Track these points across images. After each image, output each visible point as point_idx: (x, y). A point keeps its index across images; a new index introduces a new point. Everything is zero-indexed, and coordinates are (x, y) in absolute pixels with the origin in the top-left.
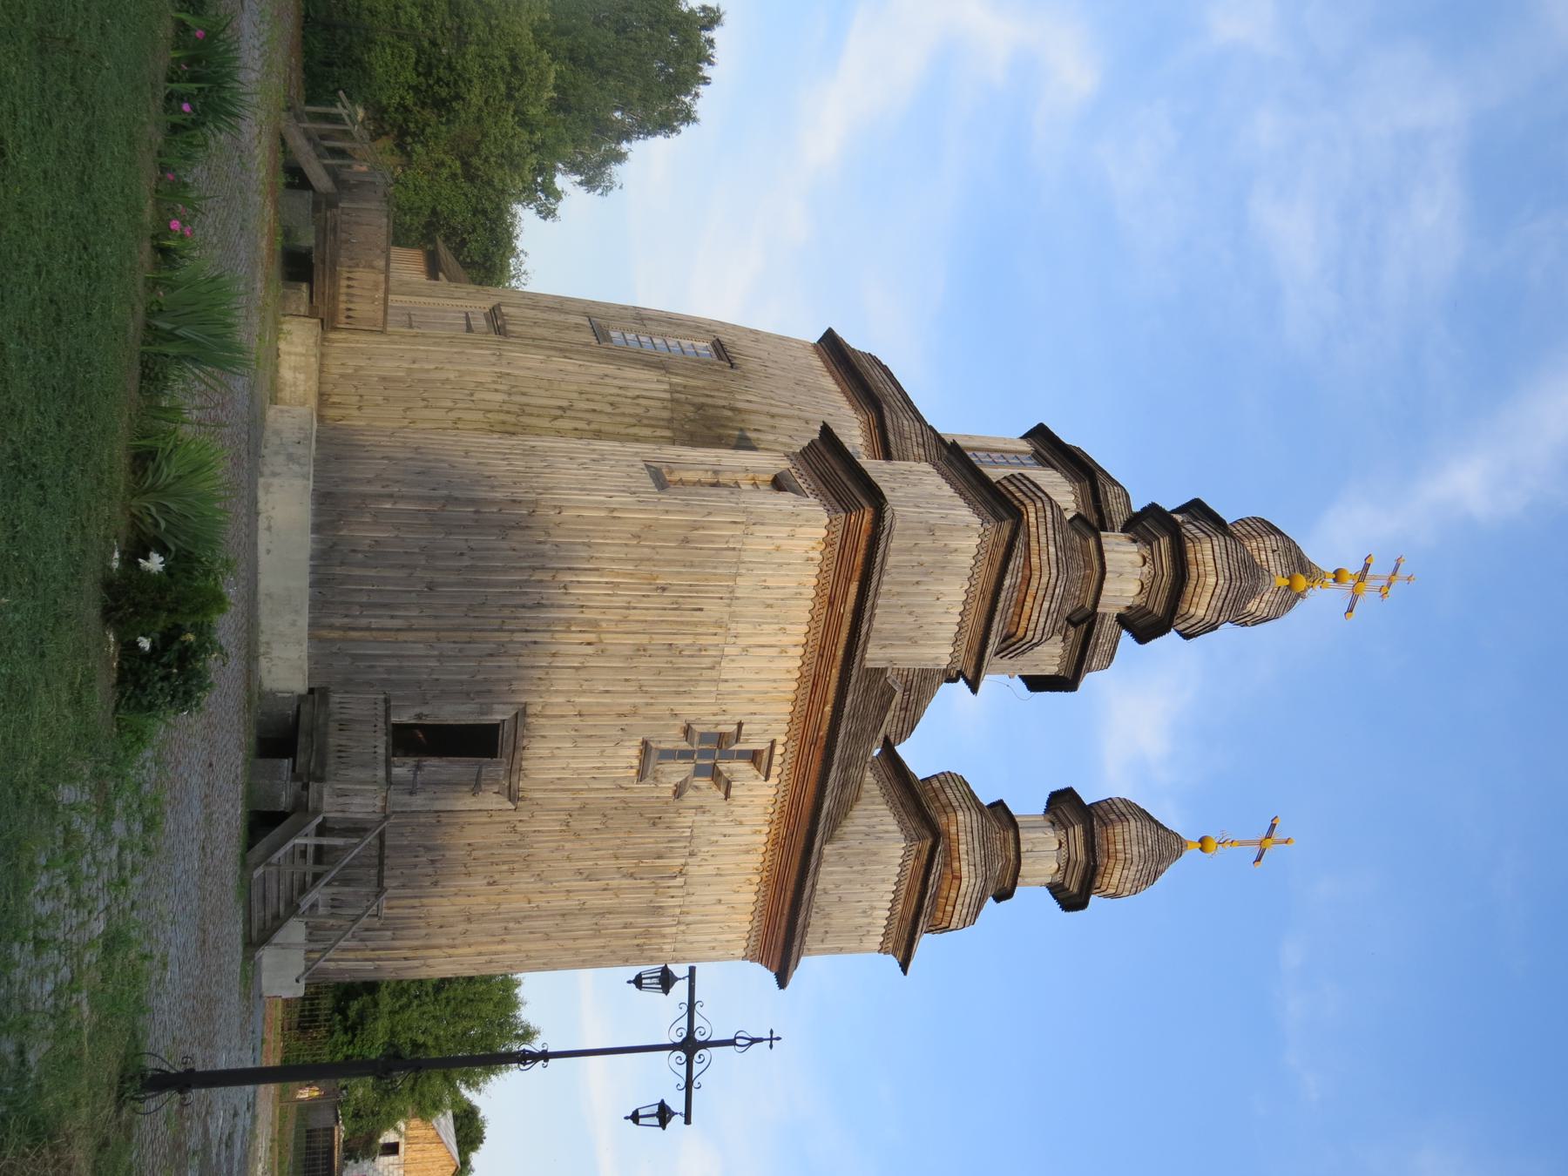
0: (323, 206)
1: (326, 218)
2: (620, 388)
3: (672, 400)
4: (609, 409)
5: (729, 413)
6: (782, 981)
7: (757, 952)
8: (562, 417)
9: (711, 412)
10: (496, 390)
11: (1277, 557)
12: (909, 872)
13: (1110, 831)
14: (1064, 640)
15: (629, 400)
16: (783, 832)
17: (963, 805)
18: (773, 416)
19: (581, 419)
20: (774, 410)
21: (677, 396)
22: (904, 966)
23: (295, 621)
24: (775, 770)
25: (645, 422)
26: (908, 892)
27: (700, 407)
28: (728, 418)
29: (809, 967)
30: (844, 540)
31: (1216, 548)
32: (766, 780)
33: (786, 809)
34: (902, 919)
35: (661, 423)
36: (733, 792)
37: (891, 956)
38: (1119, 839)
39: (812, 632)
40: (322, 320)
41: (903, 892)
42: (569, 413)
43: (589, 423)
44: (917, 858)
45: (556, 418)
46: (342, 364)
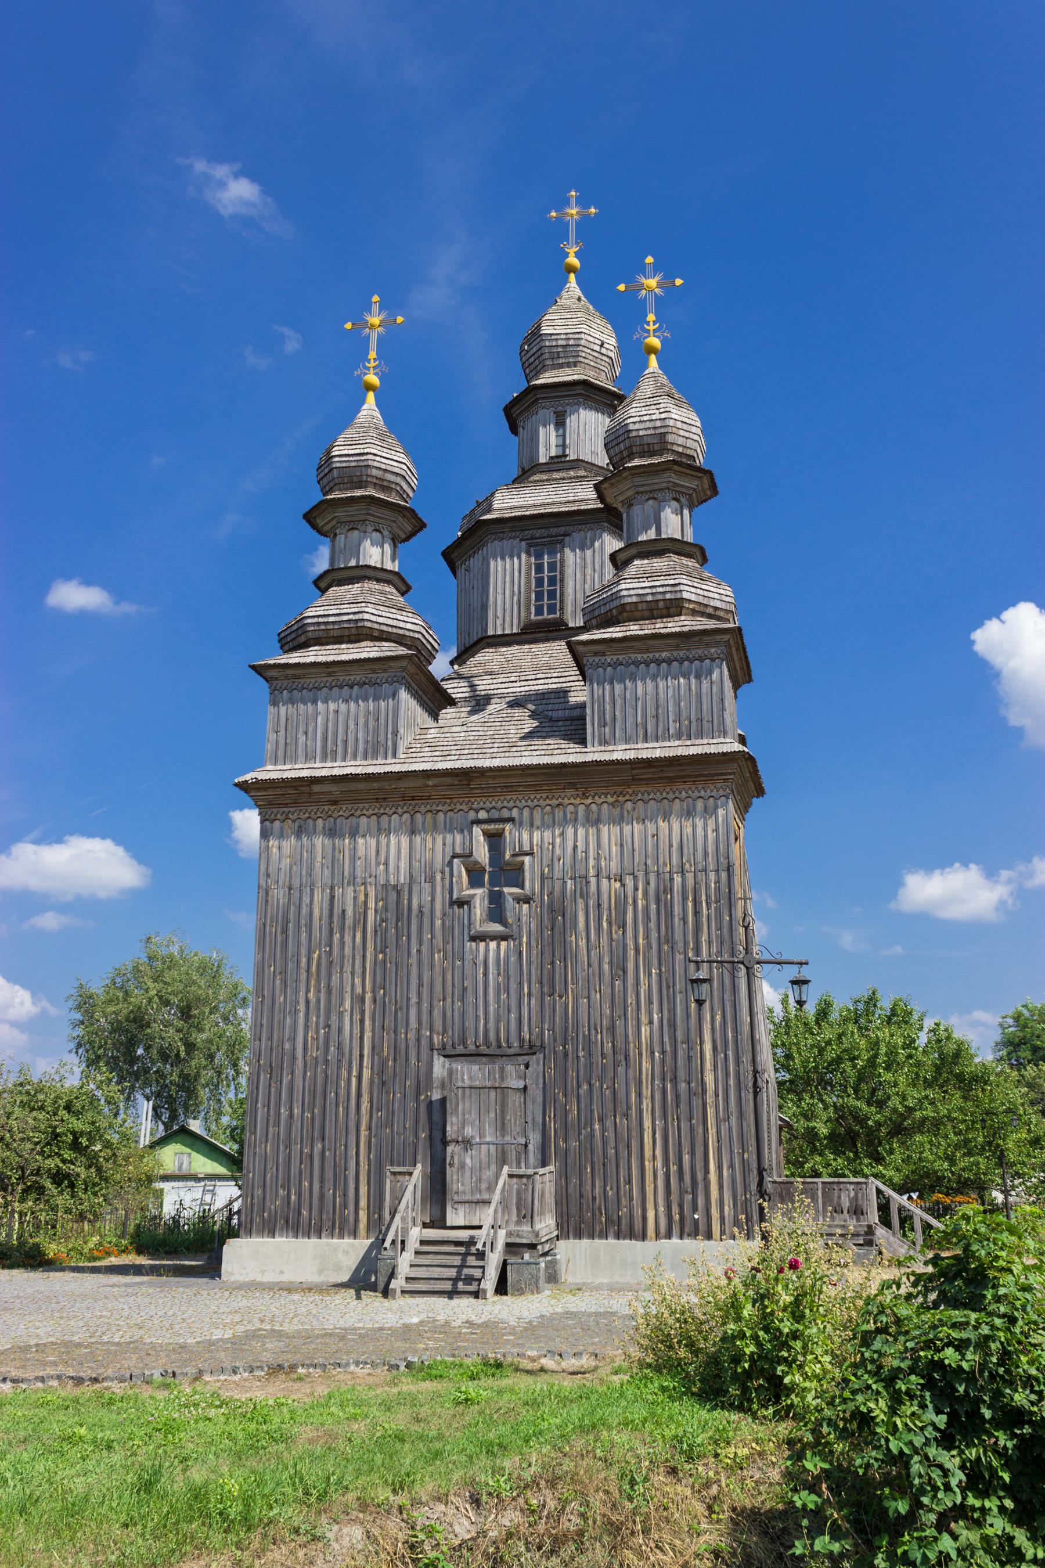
7: (719, 785)
12: (621, 657)
14: (569, 535)
16: (570, 792)
23: (344, 1251)
24: (505, 814)
26: (647, 651)
30: (280, 805)
33: (544, 795)
39: (365, 812)
41: (645, 656)
44: (603, 654)
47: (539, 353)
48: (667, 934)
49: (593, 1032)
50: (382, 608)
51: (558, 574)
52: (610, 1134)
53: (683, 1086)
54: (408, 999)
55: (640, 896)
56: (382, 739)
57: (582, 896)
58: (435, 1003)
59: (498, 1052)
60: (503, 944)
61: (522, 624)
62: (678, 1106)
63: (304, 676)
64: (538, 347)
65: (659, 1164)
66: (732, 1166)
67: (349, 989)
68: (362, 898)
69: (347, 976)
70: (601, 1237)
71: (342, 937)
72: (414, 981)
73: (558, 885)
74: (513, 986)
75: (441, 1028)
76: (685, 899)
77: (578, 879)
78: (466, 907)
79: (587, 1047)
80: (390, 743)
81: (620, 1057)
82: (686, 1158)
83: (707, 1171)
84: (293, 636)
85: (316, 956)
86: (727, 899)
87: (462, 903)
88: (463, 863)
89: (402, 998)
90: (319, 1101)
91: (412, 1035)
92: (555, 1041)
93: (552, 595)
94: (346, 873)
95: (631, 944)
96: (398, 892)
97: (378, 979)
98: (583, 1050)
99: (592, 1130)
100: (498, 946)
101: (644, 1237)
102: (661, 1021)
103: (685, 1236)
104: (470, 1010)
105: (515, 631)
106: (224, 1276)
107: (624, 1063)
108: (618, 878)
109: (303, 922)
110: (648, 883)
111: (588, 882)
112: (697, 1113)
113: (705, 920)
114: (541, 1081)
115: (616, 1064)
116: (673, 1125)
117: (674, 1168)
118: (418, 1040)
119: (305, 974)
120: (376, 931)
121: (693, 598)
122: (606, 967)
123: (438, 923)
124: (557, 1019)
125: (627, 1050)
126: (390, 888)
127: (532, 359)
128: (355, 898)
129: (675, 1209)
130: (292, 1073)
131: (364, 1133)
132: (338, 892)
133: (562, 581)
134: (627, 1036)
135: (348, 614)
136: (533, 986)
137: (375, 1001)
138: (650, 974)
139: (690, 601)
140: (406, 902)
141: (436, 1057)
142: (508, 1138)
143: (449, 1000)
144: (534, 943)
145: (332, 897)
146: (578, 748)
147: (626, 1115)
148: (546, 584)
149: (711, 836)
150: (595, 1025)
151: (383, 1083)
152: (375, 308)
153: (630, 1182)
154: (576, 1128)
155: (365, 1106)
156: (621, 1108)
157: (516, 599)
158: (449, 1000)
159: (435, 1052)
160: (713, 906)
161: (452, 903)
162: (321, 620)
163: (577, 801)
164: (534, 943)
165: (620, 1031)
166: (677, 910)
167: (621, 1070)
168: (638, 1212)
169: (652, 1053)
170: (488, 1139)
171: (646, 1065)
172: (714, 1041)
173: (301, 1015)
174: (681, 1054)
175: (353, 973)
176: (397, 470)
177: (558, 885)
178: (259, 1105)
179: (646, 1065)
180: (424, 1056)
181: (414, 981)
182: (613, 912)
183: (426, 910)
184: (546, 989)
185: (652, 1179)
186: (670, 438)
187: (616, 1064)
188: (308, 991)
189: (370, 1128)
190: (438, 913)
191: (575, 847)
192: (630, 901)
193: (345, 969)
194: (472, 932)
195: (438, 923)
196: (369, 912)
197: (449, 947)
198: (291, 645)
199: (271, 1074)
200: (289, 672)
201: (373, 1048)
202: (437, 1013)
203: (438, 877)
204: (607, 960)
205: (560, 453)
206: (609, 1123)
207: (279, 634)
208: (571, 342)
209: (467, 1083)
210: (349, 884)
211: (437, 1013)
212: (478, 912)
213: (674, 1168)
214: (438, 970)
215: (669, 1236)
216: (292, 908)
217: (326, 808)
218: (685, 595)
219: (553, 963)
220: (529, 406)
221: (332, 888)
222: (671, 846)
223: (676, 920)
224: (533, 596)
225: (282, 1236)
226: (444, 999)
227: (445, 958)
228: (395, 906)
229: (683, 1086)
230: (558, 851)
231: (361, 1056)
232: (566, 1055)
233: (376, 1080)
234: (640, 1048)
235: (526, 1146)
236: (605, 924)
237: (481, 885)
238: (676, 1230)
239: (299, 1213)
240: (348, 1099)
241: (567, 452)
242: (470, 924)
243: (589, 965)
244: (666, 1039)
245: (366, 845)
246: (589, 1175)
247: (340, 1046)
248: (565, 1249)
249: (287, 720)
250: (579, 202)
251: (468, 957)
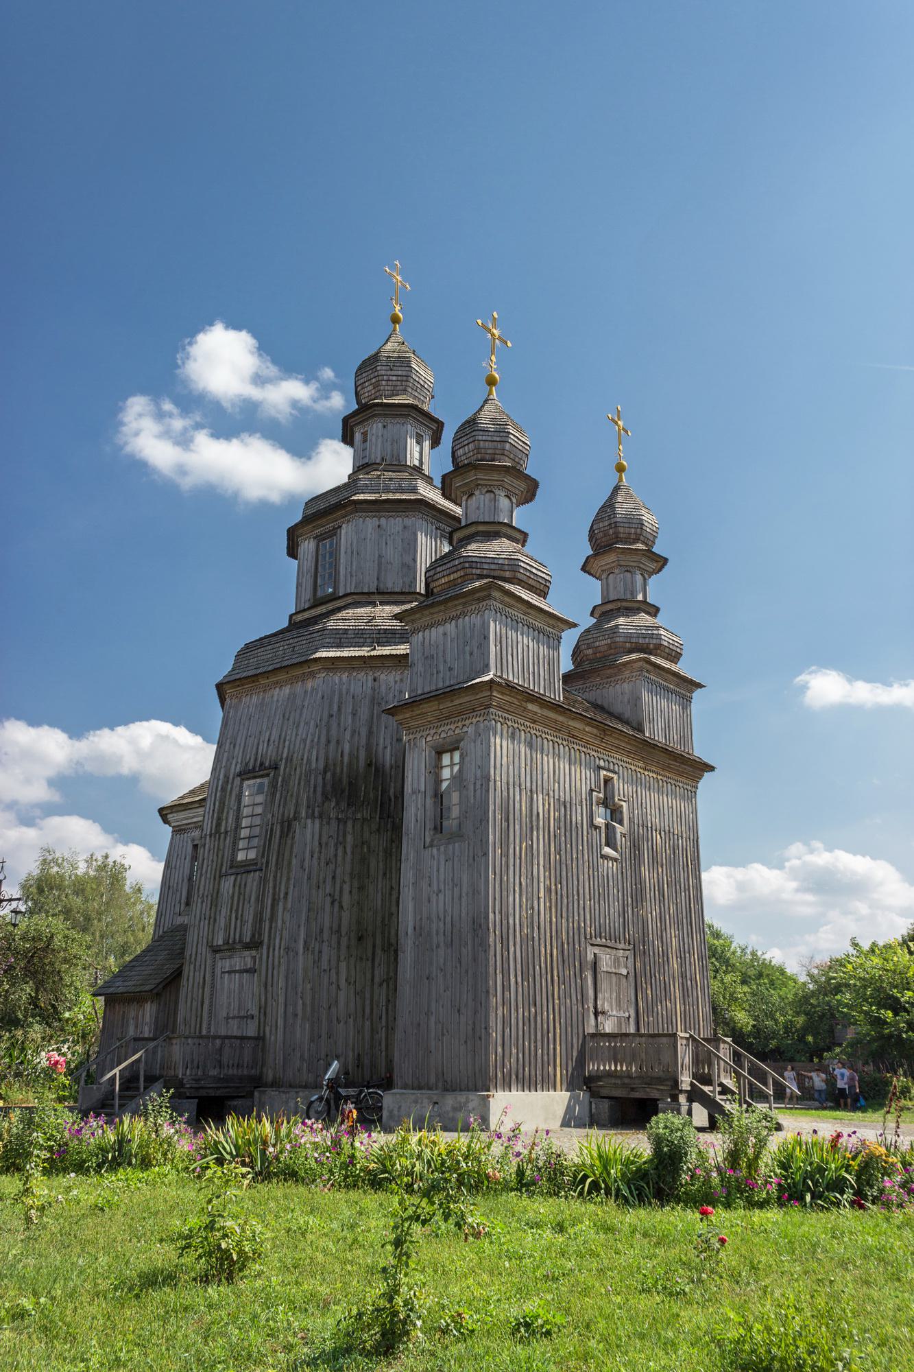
0: (182, 1090)
1: (191, 1088)
2: (312, 857)
3: (320, 817)
4: (332, 866)
5: (329, 775)
6: (712, 769)
8: (340, 903)
9: (329, 788)
10: (320, 952)
11: (395, 368)
13: (622, 535)
15: (323, 850)
17: (611, 636)
18: (328, 742)
19: (341, 888)
20: (323, 739)
21: (316, 814)
22: (699, 686)
25: (341, 839)
26: (665, 680)
27: (326, 797)
28: (334, 775)
29: (700, 751)
31: (484, 438)
34: (677, 685)
35: (341, 827)
37: (694, 695)
38: (627, 530)
40: (255, 1087)
42: (337, 897)
43: (344, 882)
45: (341, 907)
46: (299, 1071)
47: (405, 378)
63: (511, 606)
64: (404, 373)
135: (543, 572)
142: (621, 1014)
149: (691, 816)
162: (528, 568)
170: (614, 1013)
171: (675, 966)
179: (675, 966)
180: (583, 945)
189: (559, 999)
191: (642, 803)
200: (507, 599)
201: (557, 931)
208: (426, 386)
209: (605, 970)
217: (528, 724)
220: (397, 415)
235: (629, 1016)
245: (548, 762)
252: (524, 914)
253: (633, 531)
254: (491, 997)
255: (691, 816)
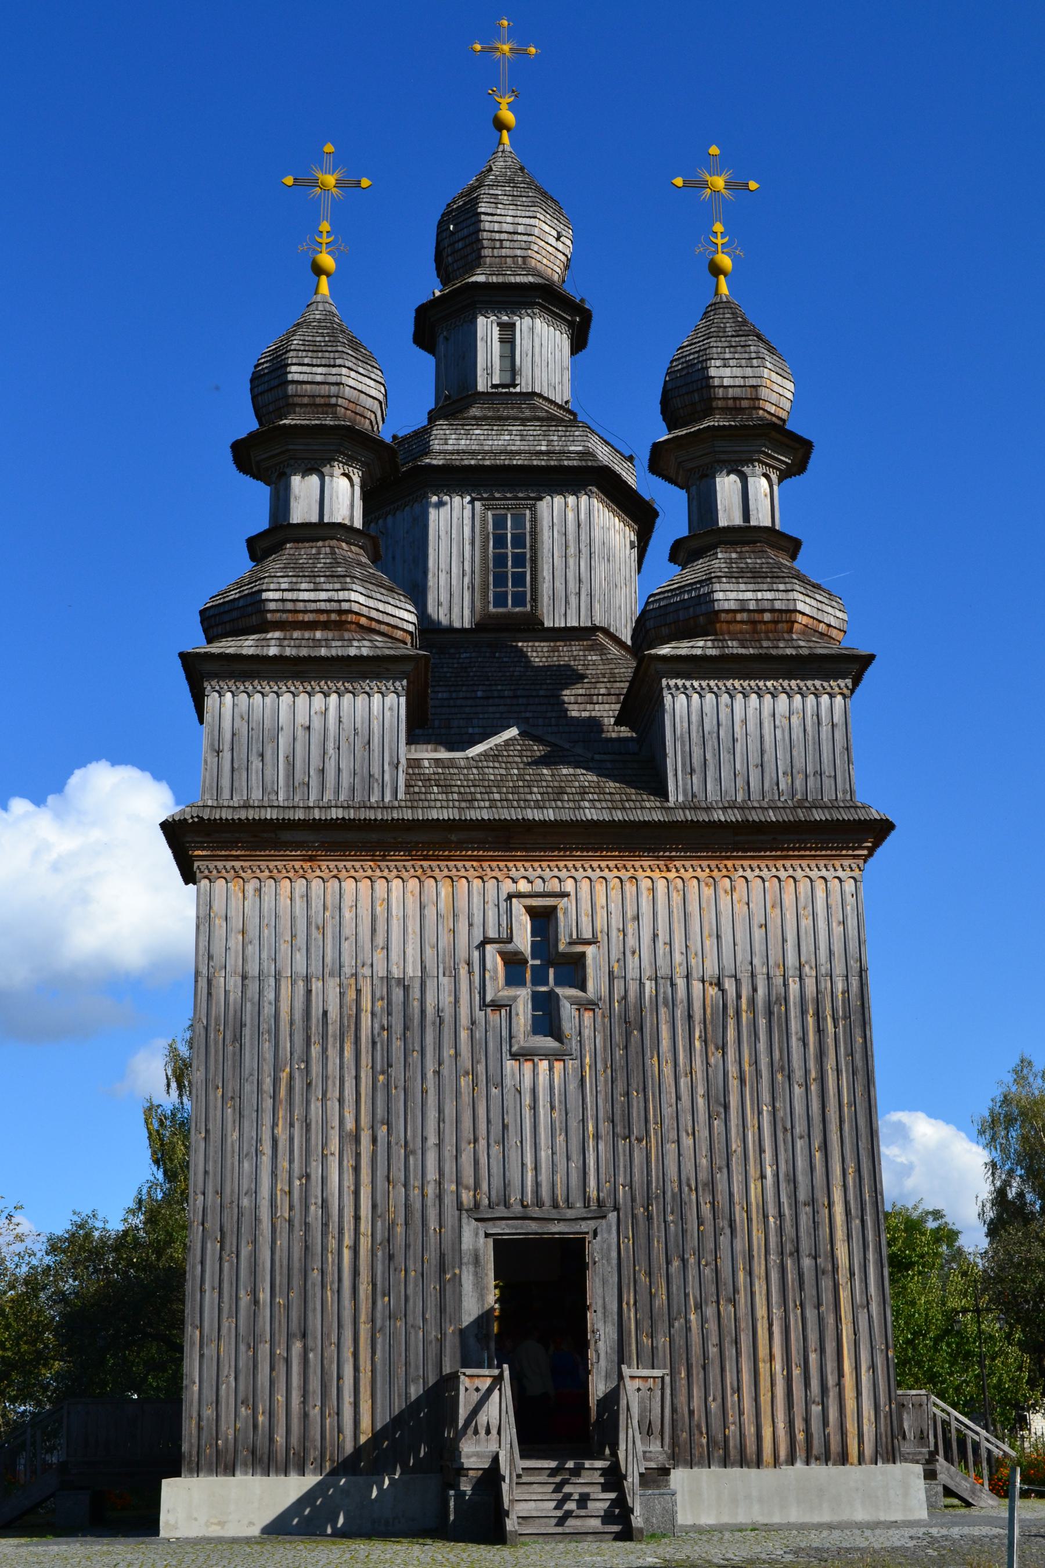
24: (554, 886)
32: (566, 895)
33: (612, 864)
36: (587, 934)
39: (352, 873)
48: (781, 1058)
49: (686, 1189)
50: (370, 586)
51: (528, 550)
52: (712, 1326)
53: (807, 1262)
54: (424, 1139)
55: (744, 1007)
56: (376, 771)
57: (666, 1005)
58: (463, 1145)
59: (554, 1214)
60: (558, 1066)
61: (477, 617)
62: (801, 1288)
65: (778, 1366)
66: (873, 1367)
67: (336, 1123)
68: (352, 995)
69: (333, 1106)
70: (700, 1464)
71: (324, 1050)
72: (432, 1115)
73: (633, 987)
74: (574, 1124)
75: (471, 1181)
76: (803, 1012)
77: (661, 981)
78: (503, 1011)
79: (677, 1210)
80: (387, 777)
81: (723, 1223)
82: (813, 1357)
83: (841, 1374)
84: (235, 614)
85: (284, 1076)
86: (859, 1016)
87: (496, 1006)
88: (501, 953)
89: (414, 1137)
90: (297, 1282)
91: (431, 1190)
92: (633, 1200)
93: (519, 580)
94: (328, 959)
95: (733, 1070)
96: (406, 989)
97: (379, 1111)
98: (672, 1213)
99: (687, 1321)
100: (551, 1069)
101: (759, 1464)
102: (777, 1175)
103: (813, 1460)
104: (514, 1156)
105: (467, 625)
106: (163, 1533)
107: (728, 1231)
108: (715, 981)
109: (264, 1026)
110: (755, 990)
111: (673, 985)
112: (827, 1297)
113: (830, 1041)
114: (614, 1254)
115: (717, 1234)
116: (796, 1316)
117: (796, 1372)
118: (440, 1197)
119: (270, 1102)
120: (374, 1043)
121: (807, 610)
122: (701, 1102)
123: (464, 1035)
124: (636, 1170)
125: (731, 1213)
126: (393, 982)
127: (460, 245)
128: (342, 995)
129: (799, 1425)
130: (255, 1242)
131: (364, 1329)
132: (316, 986)
133: (534, 561)
134: (731, 1195)
136: (601, 1126)
137: (374, 1140)
138: (760, 1113)
139: (804, 614)
140: (417, 1004)
141: (464, 1221)
143: (482, 1143)
144: (600, 1066)
145: (309, 992)
146: (651, 802)
147: (734, 1302)
148: (510, 563)
149: (838, 930)
150: (688, 1179)
151: (391, 1257)
152: (328, 161)
153: (739, 1390)
154: (666, 1318)
155: (364, 1288)
156: (726, 1291)
157: (467, 580)
158: (482, 1143)
159: (464, 1215)
160: (841, 1023)
161: (484, 1005)
163: (656, 875)
164: (600, 1066)
165: (721, 1186)
166: (794, 1026)
167: (724, 1240)
168: (750, 1430)
169: (765, 1217)
172: (846, 1203)
173: (266, 1160)
174: (804, 1220)
175: (341, 1100)
176: (374, 393)
177: (633, 987)
178: (207, 1286)
179: (757, 1235)
181: (432, 1115)
182: (709, 1027)
183: (447, 1015)
184: (619, 1129)
185: (769, 1384)
186: (764, 393)
187: (717, 1234)
188: (275, 1125)
189: (373, 1321)
190: (464, 1020)
192: (731, 1012)
193: (329, 1095)
194: (514, 1049)
195: (464, 1035)
196: (363, 1015)
197: (481, 1068)
198: (228, 627)
199: (222, 1242)
201: (374, 1206)
202: (467, 1158)
203: (463, 971)
204: (701, 1090)
205: (508, 381)
206: (710, 1311)
207: (202, 612)
208: (521, 229)
210: (332, 975)
211: (467, 1158)
212: (522, 1021)
213: (796, 1372)
214: (466, 1099)
215: (791, 1460)
216: (249, 1005)
218: (800, 606)
219: (627, 1094)
221: (307, 979)
222: (784, 940)
223: (794, 1042)
224: (491, 578)
225: (246, 1473)
226: (476, 1140)
227: (475, 1084)
228: (401, 1007)
229: (807, 1262)
230: (631, 941)
231: (357, 1218)
232: (649, 1218)
233: (379, 1254)
234: (748, 1212)
236: (697, 1044)
237: (522, 983)
238: (800, 1453)
239: (271, 1439)
240: (340, 1280)
241: (517, 382)
242: (511, 1038)
243: (678, 1098)
244: (784, 1199)
246: (684, 1382)
247: (325, 1204)
248: (679, 1477)
249: (233, 735)
250: (512, 34)
251: (508, 1082)
252: (282, 1185)
253: (696, 397)
254: (189, 1329)
255: (838, 930)
